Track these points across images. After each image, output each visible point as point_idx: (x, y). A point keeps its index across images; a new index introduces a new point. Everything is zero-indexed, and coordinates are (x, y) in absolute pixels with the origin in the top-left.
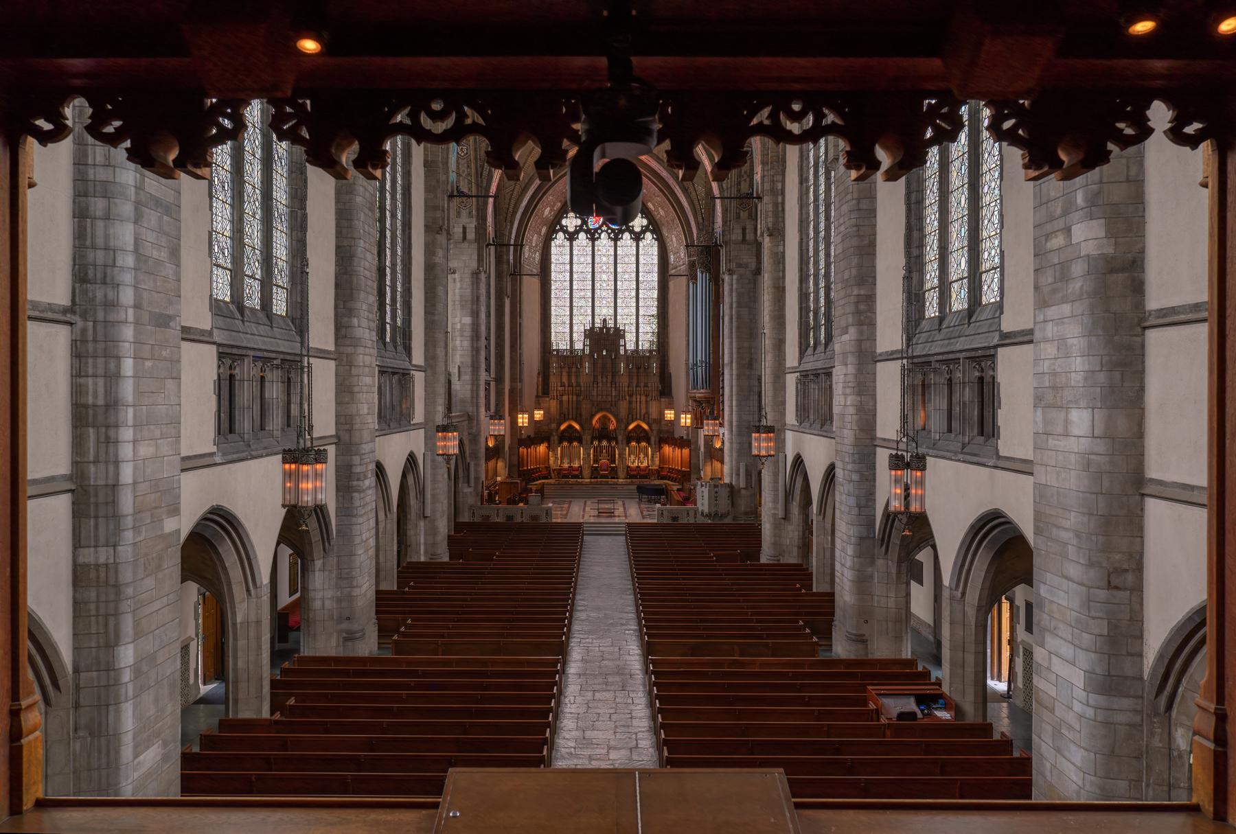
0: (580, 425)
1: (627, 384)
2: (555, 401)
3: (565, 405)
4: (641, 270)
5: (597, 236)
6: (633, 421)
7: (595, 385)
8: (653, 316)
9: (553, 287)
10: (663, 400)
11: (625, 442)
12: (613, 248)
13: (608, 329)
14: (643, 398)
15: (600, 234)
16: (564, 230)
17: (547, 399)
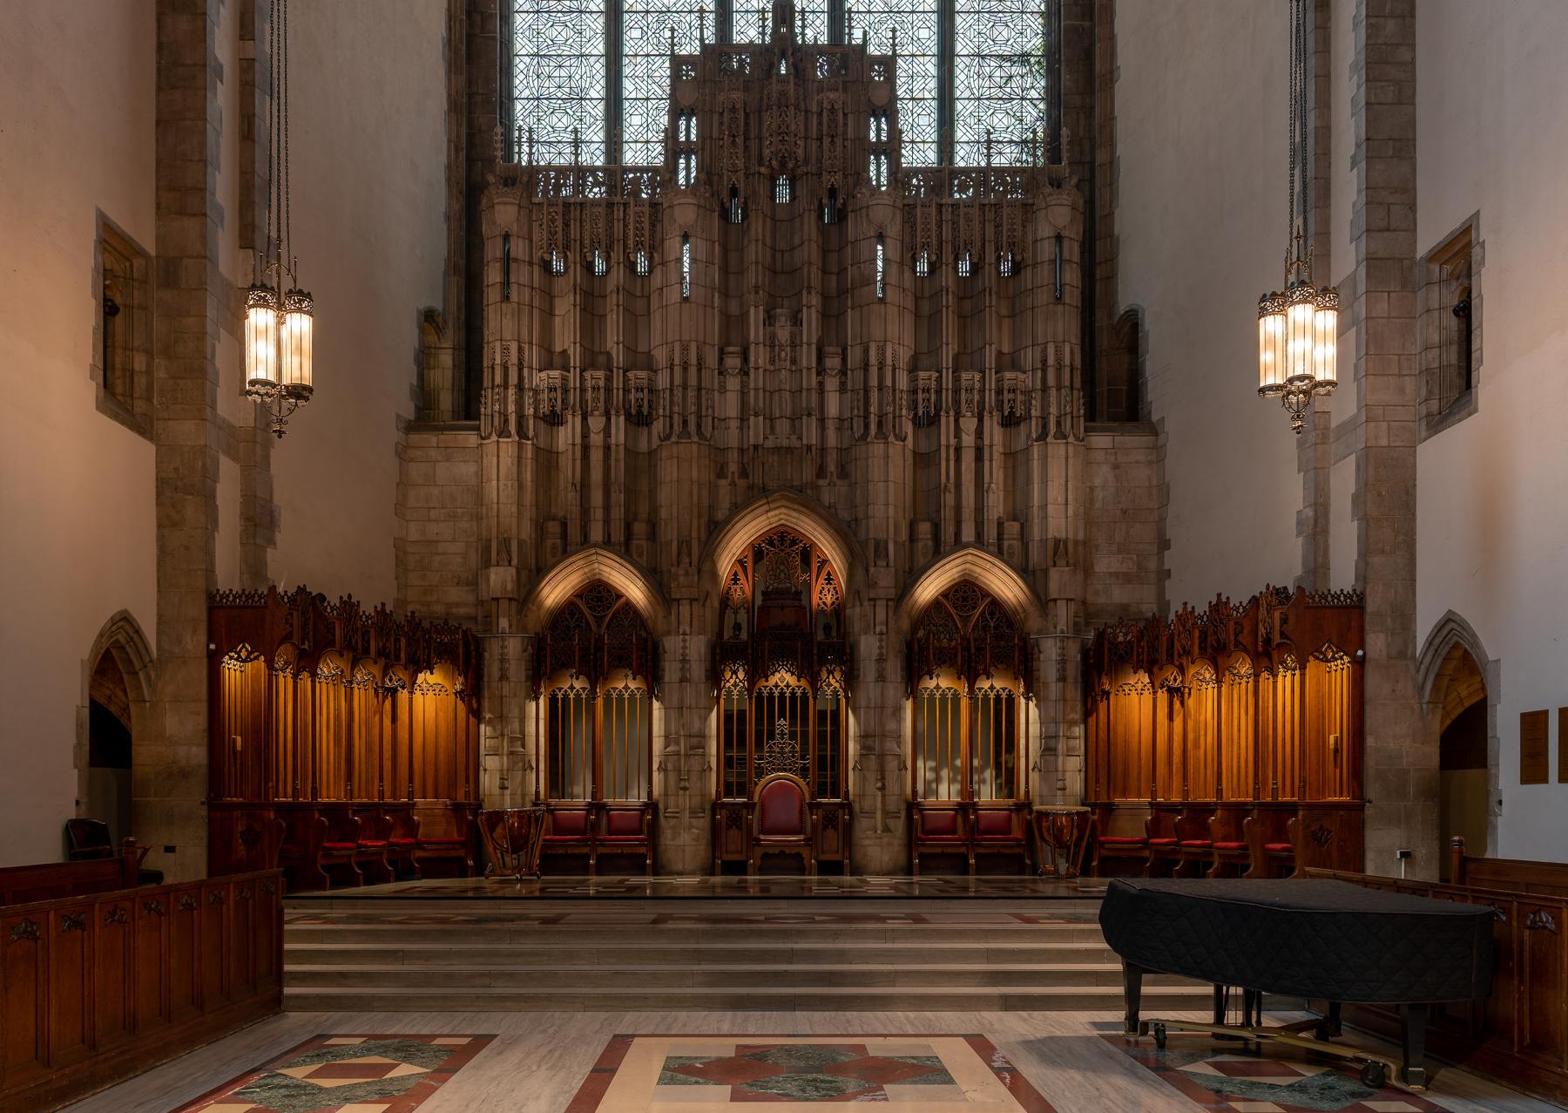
0: (653, 576)
1: (905, 355)
2: (508, 447)
3: (568, 470)
6: (938, 553)
7: (733, 362)
8: (1023, 58)
10: (1101, 441)
11: (894, 669)
13: (802, 56)
14: (995, 433)
17: (472, 439)
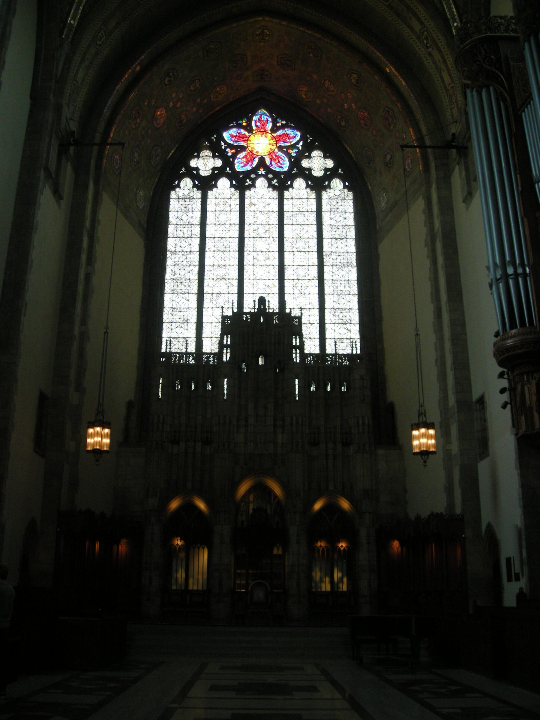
4: (325, 234)
5: (249, 182)
9: (169, 262)
12: (276, 202)
15: (254, 181)
16: (193, 174)
